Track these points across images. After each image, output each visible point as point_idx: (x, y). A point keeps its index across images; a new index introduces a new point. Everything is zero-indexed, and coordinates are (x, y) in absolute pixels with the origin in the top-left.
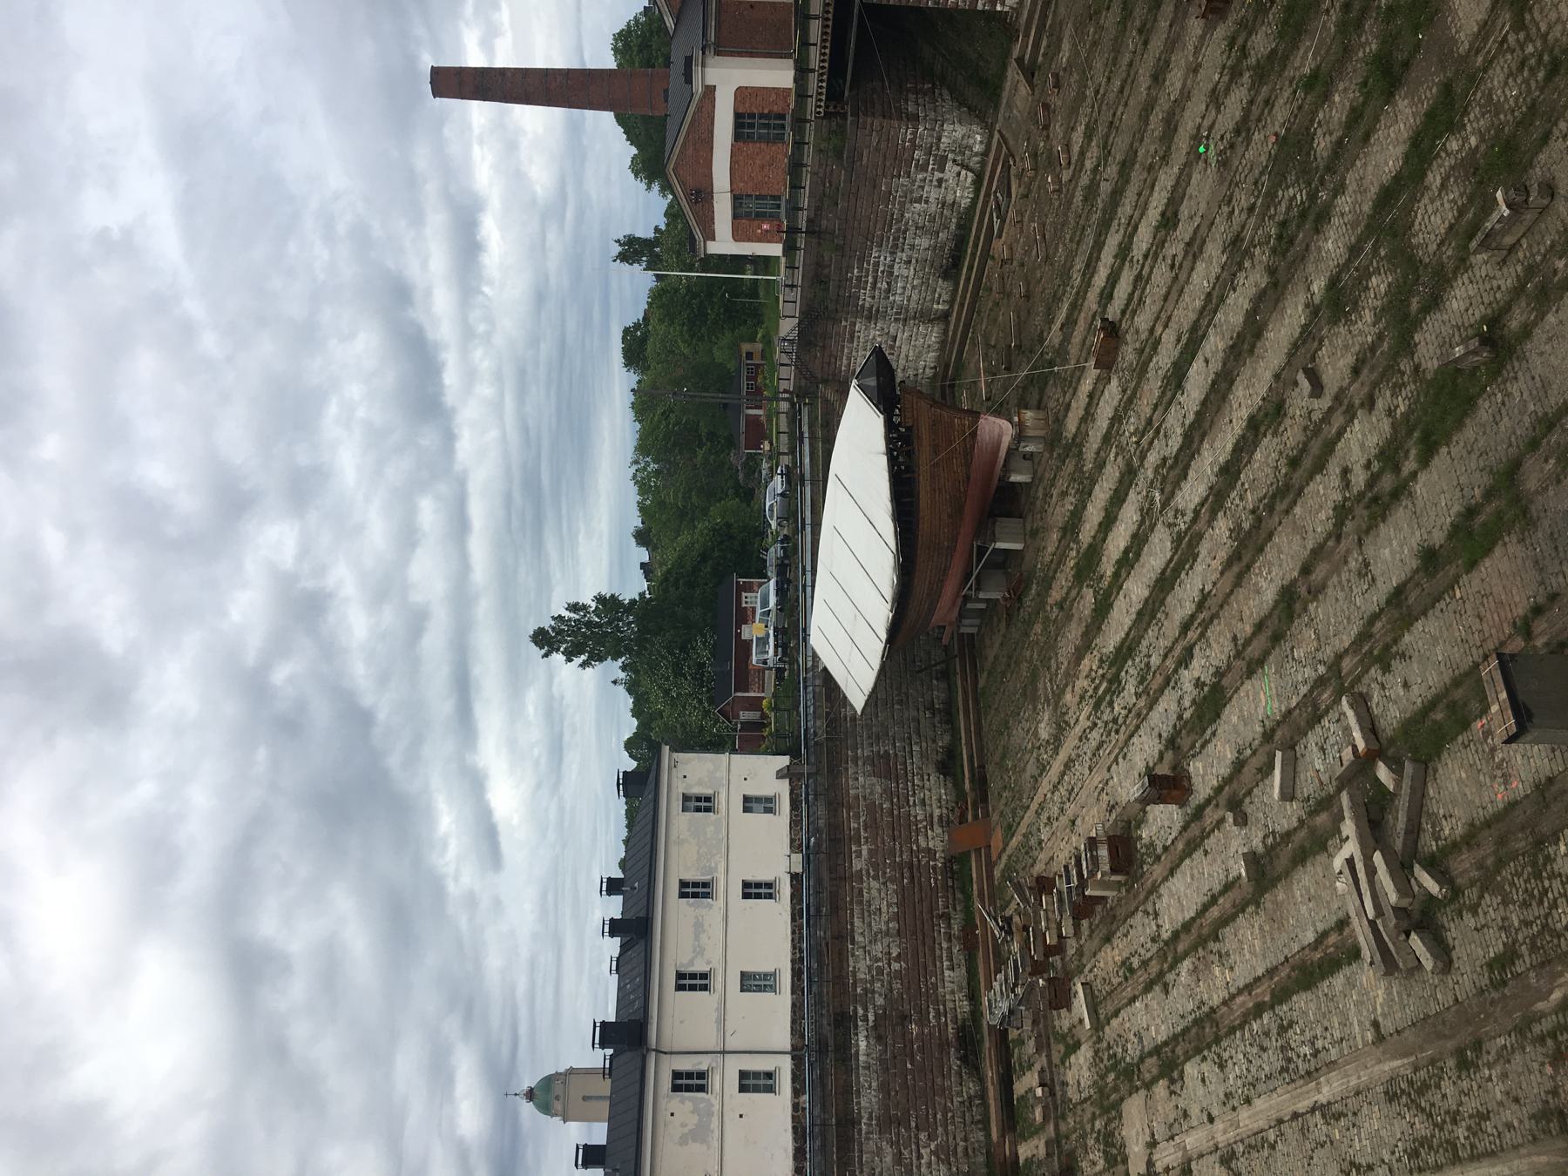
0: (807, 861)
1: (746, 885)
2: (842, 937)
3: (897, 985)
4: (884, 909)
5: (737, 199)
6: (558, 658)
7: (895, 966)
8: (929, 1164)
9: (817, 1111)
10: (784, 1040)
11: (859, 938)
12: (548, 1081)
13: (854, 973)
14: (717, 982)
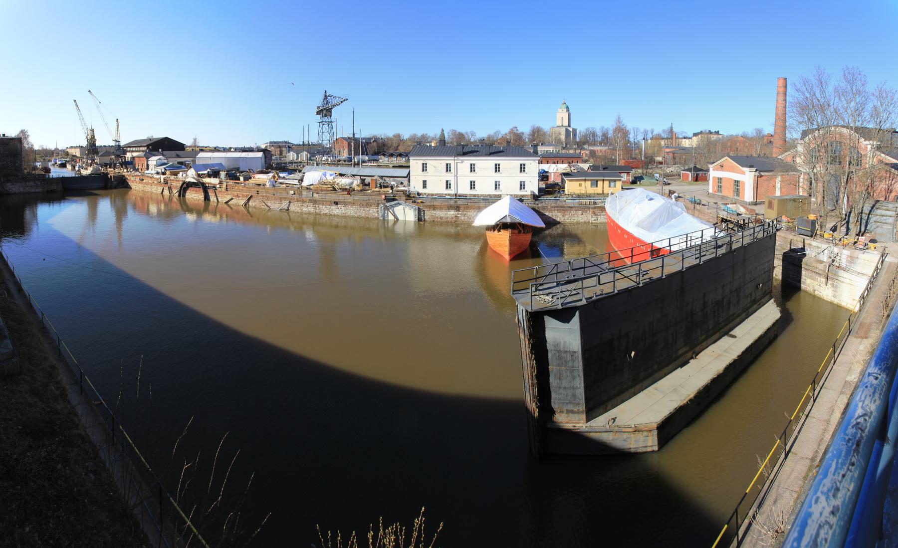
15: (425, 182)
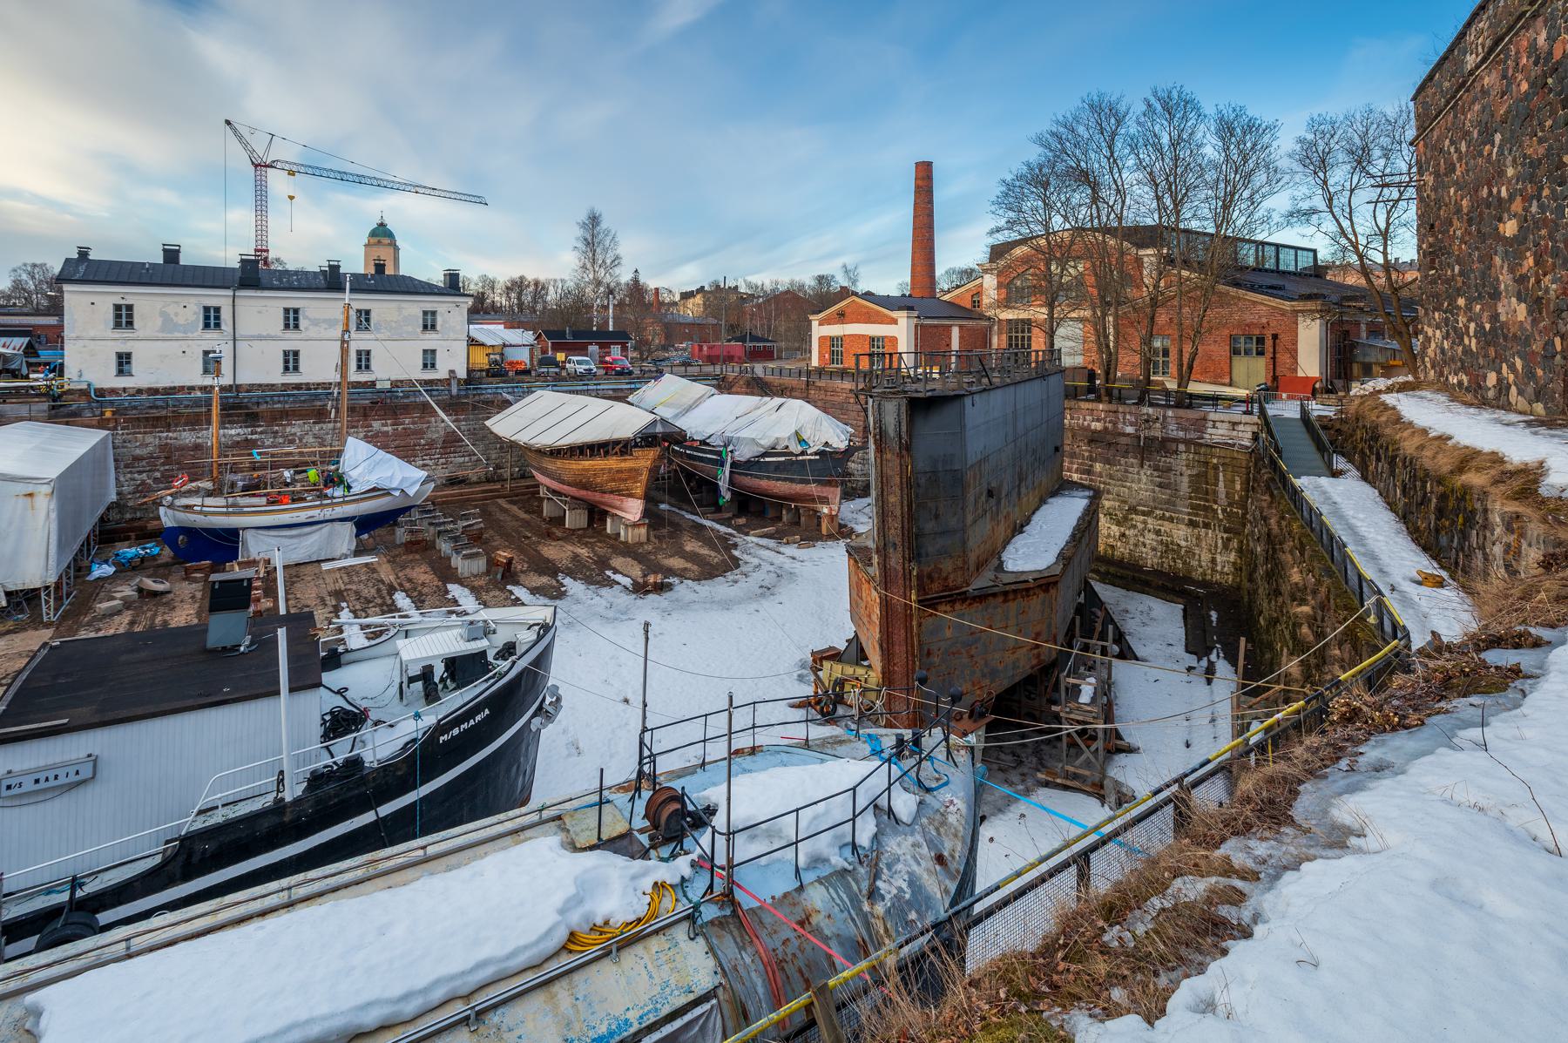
5: (842, 338)
10: (245, 378)
14: (291, 334)
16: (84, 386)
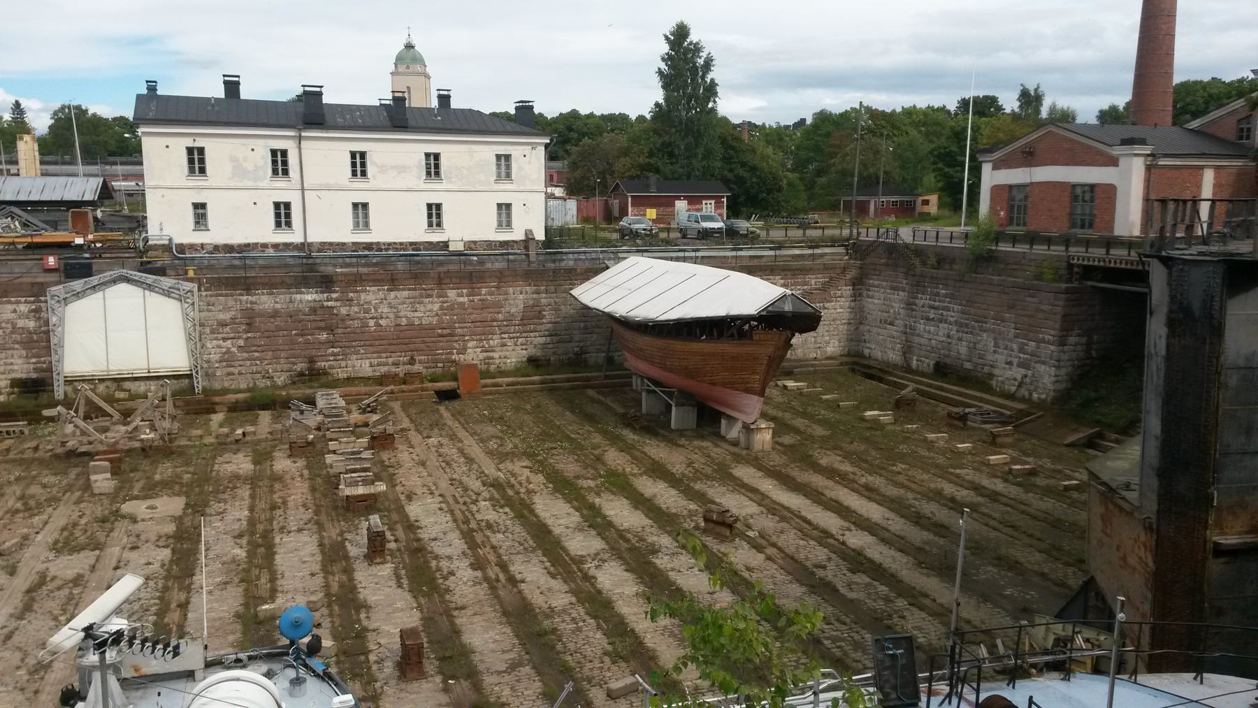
0: (459, 254)
1: (439, 206)
2: (393, 282)
3: (356, 323)
4: (416, 314)
6: (665, 48)
7: (372, 323)
8: (220, 347)
9: (261, 262)
10: (315, 236)
11: (393, 294)
12: (419, 60)
13: (365, 291)
14: (359, 183)
15: (200, 208)
16: (166, 242)
